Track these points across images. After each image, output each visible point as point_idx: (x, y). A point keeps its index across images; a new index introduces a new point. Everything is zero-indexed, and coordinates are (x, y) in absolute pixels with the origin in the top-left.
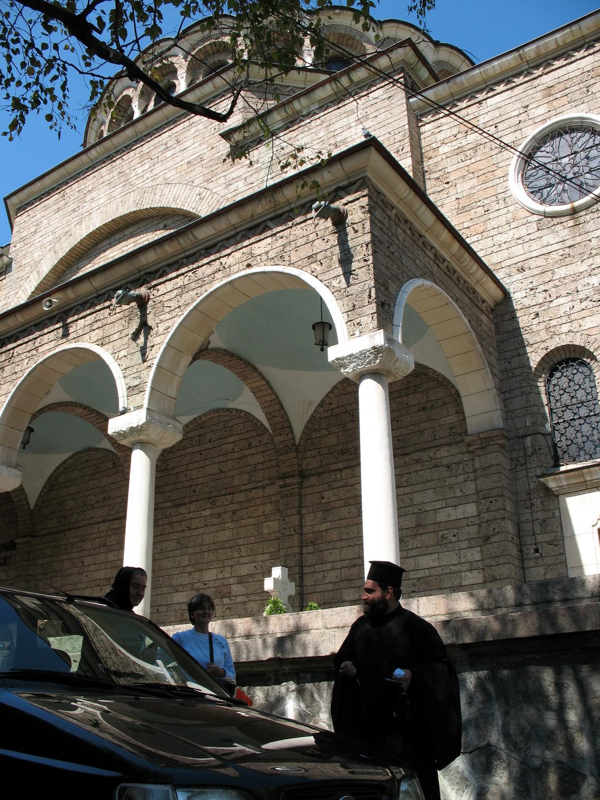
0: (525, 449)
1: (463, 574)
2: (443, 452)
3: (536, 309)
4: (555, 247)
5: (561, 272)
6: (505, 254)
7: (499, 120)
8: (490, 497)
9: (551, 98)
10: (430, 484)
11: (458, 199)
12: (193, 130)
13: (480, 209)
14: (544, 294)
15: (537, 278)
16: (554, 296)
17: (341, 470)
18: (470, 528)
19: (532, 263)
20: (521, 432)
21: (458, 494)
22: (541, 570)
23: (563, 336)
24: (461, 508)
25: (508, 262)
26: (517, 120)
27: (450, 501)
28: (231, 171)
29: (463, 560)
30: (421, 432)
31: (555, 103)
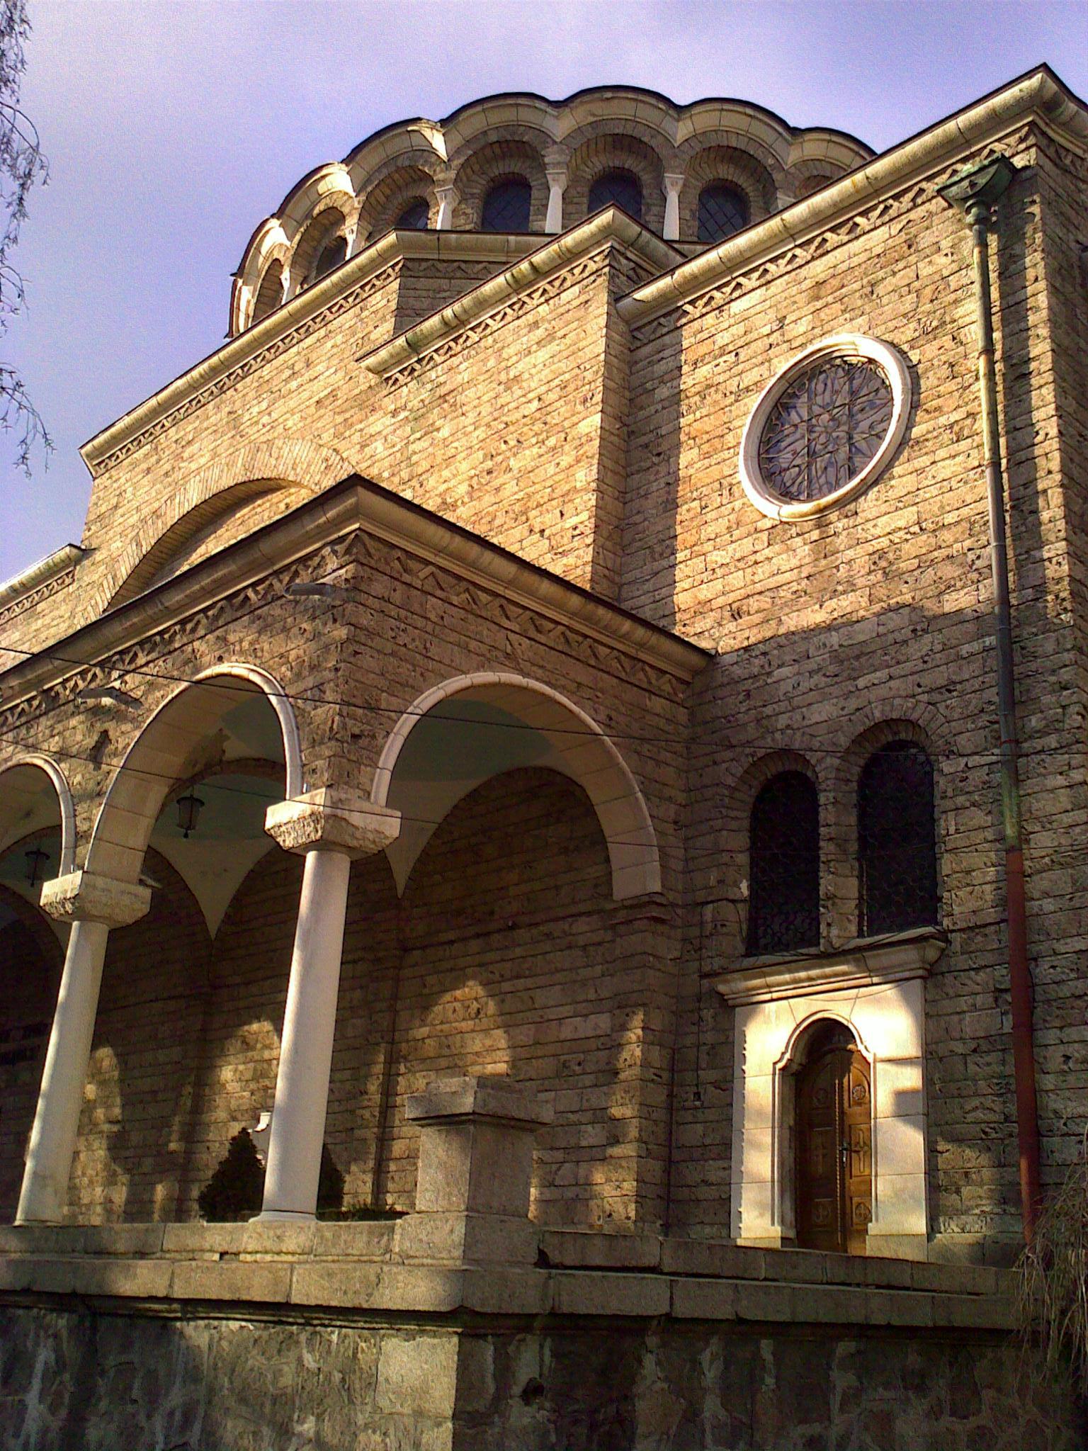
0: (702, 923)
1: (583, 1127)
2: (581, 926)
3: (748, 685)
6: (718, 585)
7: (741, 343)
8: (626, 1006)
9: (819, 304)
10: (559, 977)
11: (669, 484)
12: (329, 344)
13: (696, 503)
14: (762, 660)
15: (755, 630)
16: (774, 663)
17: (452, 942)
18: (601, 1053)
19: (754, 604)
20: (701, 896)
21: (592, 996)
22: (700, 1128)
23: (778, 735)
25: (721, 601)
27: (580, 1007)
28: (371, 419)
29: (585, 1105)
30: (557, 888)
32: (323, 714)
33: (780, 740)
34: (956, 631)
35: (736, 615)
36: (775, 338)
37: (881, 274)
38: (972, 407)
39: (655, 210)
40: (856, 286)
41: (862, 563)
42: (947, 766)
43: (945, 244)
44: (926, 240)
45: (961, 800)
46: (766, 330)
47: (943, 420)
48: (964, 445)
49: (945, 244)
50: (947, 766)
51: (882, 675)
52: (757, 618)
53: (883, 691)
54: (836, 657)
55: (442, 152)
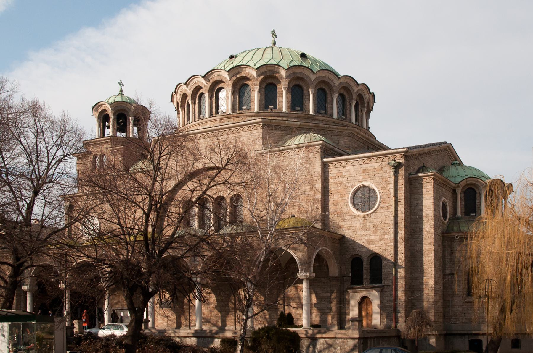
3: (351, 242)
4: (358, 225)
5: (359, 233)
7: (348, 176)
9: (364, 174)
19: (352, 228)
24: (326, 294)
25: (346, 226)
26: (353, 178)
31: (365, 176)
32: (223, 211)
33: (357, 253)
34: (387, 241)
35: (349, 229)
36: (355, 178)
37: (376, 173)
38: (391, 204)
39: (307, 97)
40: (371, 173)
41: (371, 226)
42: (385, 262)
43: (388, 172)
44: (385, 169)
45: (387, 267)
46: (354, 175)
47: (386, 205)
48: (389, 210)
49: (388, 172)
50: (385, 262)
51: (374, 246)
52: (353, 231)
53: (375, 248)
54: (367, 241)
55: (255, 75)
